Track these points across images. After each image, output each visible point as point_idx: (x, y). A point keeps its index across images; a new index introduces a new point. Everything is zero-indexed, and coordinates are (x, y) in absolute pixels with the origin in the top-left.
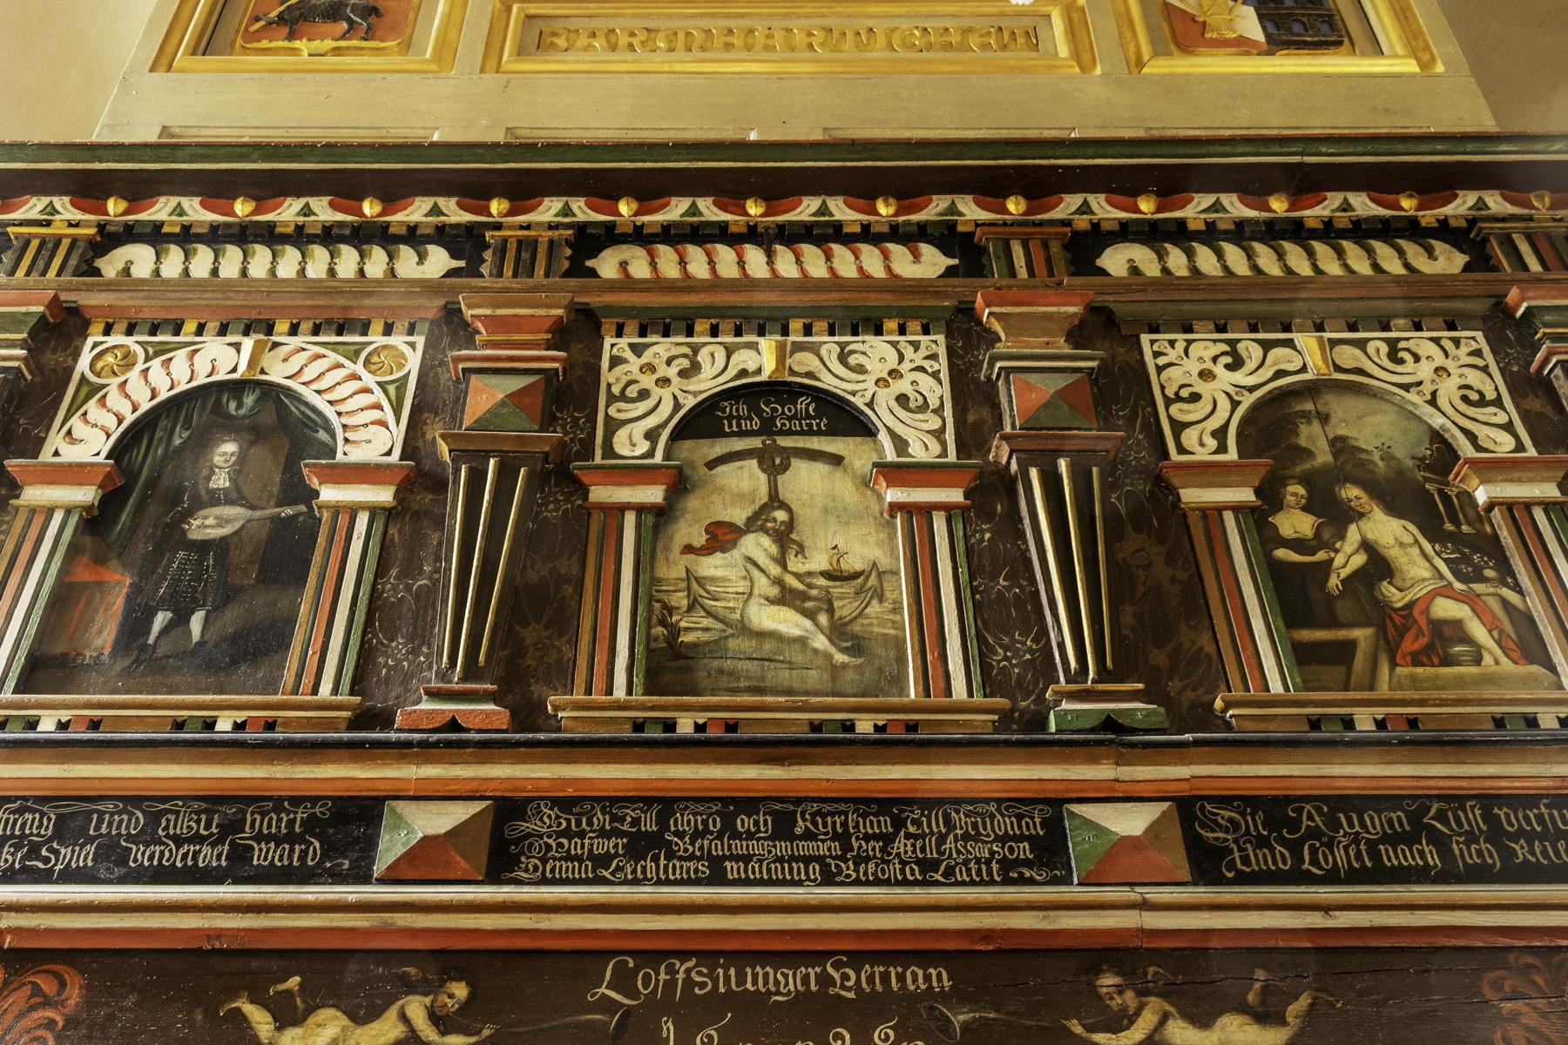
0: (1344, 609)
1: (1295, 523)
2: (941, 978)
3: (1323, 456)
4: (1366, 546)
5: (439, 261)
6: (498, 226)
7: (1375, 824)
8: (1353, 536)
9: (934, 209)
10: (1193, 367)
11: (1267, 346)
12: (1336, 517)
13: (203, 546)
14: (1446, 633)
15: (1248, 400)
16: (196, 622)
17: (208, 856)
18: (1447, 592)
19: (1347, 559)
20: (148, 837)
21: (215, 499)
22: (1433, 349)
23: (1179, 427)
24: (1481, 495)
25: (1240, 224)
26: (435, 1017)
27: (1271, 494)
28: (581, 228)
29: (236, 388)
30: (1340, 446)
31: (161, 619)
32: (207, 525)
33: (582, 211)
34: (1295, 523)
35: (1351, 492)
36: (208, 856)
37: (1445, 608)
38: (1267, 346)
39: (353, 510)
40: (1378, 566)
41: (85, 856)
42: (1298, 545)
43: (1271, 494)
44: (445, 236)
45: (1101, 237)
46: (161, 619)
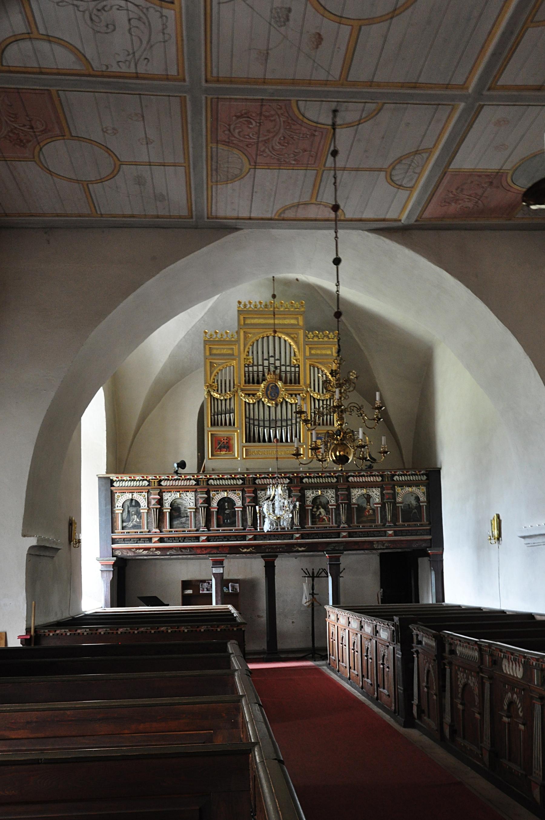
0: (317, 518)
1: (315, 510)
2: (284, 546)
3: (318, 503)
4: (320, 512)
5: (241, 482)
6: (246, 478)
7: (314, 535)
8: (319, 511)
9: (288, 475)
10: (309, 494)
11: (316, 491)
12: (318, 509)
13: (227, 514)
14: (324, 519)
15: (313, 497)
16: (229, 521)
17: (235, 539)
18: (325, 516)
19: (318, 513)
20: (230, 538)
21: (227, 509)
22: (330, 492)
23: (307, 500)
24: (330, 507)
25: (317, 476)
26: (253, 549)
27: (313, 507)
28: (254, 478)
29: (225, 497)
30: (320, 502)
31: (226, 521)
32: (227, 512)
33: (254, 476)
34: (315, 510)
35: (320, 507)
36: (235, 539)
37: (324, 517)
38: (316, 491)
39: (239, 511)
40: (320, 514)
41: (226, 540)
42: (315, 512)
43: (313, 507)
44: (241, 478)
45: (303, 478)
46: (226, 521)
